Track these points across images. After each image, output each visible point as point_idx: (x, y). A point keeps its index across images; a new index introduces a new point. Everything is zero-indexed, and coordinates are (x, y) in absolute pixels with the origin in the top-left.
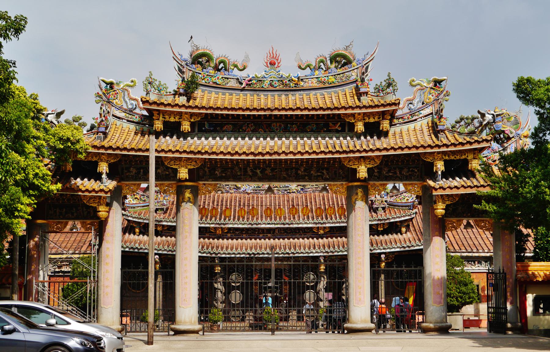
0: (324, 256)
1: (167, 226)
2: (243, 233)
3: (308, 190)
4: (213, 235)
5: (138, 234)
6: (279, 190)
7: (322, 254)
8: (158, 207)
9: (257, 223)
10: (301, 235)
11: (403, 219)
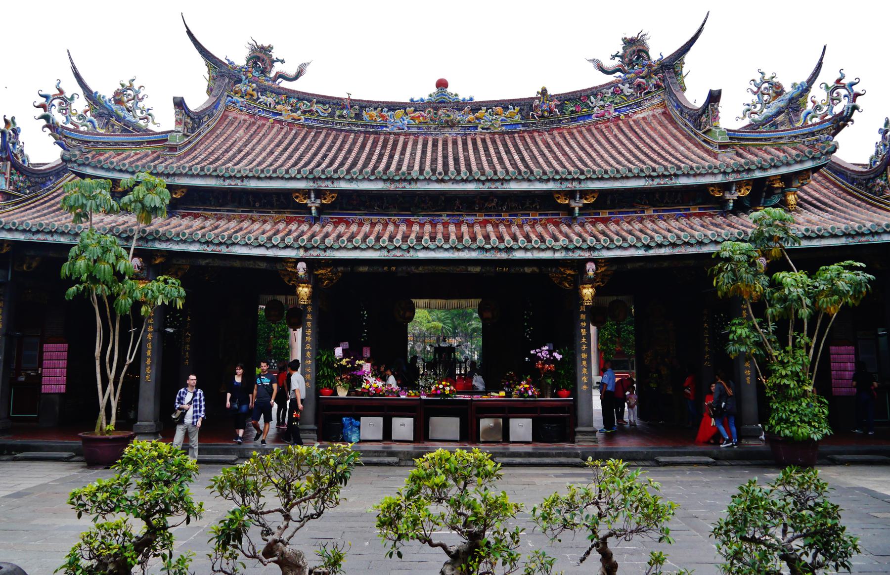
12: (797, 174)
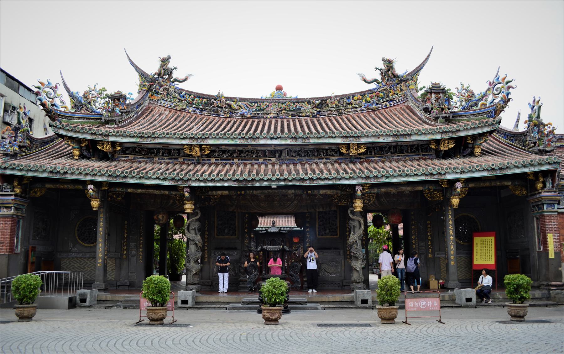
0: (361, 185)
1: (121, 144)
2: (234, 157)
3: (327, 113)
4: (190, 160)
5: (77, 157)
6: (288, 114)
7: (360, 181)
8: (108, 119)
9: (255, 137)
10: (322, 159)
11: (479, 131)
12: (482, 135)
